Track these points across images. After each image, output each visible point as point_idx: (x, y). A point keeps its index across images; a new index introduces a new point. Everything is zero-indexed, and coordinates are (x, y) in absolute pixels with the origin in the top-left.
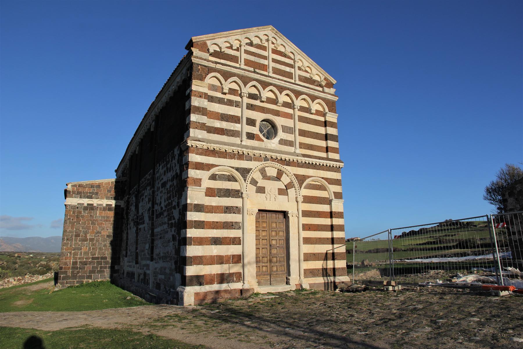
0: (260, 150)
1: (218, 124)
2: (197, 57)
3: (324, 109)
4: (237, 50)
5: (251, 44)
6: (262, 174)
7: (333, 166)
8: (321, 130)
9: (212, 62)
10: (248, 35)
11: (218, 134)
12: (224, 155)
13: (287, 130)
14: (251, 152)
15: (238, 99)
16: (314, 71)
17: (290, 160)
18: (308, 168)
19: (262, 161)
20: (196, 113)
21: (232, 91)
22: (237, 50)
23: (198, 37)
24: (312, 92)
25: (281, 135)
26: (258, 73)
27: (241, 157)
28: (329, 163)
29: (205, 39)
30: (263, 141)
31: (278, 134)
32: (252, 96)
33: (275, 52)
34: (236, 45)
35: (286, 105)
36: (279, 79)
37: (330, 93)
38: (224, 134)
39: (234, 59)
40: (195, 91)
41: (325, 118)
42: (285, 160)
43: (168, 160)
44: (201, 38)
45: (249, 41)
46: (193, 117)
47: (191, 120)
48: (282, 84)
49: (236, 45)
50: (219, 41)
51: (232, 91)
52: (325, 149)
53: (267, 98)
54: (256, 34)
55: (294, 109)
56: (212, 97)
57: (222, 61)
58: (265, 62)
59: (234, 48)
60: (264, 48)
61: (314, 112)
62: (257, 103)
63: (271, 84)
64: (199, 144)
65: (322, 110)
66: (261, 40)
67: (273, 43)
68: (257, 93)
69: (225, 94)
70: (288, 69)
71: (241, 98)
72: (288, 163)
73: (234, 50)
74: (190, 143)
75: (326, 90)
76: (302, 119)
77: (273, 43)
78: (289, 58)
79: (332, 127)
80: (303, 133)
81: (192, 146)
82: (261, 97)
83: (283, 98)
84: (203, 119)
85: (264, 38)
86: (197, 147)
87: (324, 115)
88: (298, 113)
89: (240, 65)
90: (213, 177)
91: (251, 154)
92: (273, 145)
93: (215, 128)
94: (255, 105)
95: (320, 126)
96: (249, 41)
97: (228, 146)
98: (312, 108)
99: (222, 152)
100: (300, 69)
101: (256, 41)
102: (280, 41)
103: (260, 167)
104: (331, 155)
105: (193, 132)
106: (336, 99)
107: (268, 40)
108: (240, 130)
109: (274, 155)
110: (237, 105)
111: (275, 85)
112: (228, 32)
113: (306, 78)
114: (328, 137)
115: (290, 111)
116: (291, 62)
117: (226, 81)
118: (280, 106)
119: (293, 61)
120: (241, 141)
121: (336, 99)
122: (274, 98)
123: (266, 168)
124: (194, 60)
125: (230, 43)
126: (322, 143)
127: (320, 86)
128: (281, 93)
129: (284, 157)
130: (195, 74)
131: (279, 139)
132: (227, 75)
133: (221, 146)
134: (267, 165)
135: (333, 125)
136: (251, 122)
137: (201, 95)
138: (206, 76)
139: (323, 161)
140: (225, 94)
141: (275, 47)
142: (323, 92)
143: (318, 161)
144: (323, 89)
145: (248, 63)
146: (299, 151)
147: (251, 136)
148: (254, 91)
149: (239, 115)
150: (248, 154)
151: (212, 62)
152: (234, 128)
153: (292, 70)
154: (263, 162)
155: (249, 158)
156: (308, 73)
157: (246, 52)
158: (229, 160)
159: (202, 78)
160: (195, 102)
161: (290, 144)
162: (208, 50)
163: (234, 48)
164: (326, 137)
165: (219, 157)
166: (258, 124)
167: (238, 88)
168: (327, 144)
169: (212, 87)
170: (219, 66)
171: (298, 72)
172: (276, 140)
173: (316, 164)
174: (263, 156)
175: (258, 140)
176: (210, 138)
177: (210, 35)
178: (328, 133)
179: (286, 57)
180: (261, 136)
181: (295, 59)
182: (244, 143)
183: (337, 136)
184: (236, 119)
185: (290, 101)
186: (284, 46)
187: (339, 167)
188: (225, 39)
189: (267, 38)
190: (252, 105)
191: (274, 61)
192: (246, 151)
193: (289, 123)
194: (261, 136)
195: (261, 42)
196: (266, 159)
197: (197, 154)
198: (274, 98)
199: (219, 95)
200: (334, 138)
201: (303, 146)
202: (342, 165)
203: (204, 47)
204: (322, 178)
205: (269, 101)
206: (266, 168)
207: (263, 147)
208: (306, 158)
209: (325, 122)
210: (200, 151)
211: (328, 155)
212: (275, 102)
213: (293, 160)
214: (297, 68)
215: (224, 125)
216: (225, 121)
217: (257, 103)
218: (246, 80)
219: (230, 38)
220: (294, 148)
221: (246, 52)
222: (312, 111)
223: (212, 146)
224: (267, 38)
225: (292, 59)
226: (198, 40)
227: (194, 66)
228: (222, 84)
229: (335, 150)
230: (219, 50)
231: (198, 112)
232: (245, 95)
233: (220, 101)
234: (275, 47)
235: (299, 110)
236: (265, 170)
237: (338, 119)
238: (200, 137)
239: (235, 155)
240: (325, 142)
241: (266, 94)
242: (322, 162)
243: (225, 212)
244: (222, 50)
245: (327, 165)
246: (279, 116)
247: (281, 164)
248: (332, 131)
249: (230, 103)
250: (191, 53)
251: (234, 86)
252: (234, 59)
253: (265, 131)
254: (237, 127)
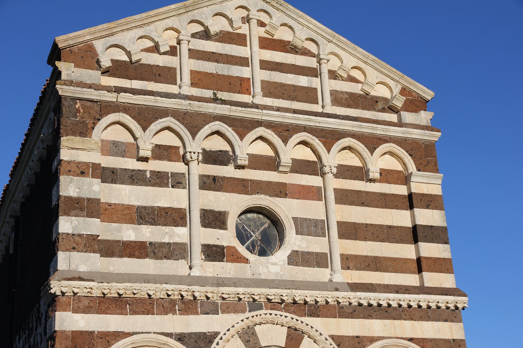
0: (235, 285)
1: (129, 233)
2: (71, 83)
3: (404, 164)
4: (173, 51)
5: (206, 35)
7: (438, 308)
8: (401, 218)
9: (109, 89)
10: (196, 14)
11: (131, 256)
12: (145, 306)
13: (308, 227)
14: (214, 293)
15: (179, 167)
16: (373, 76)
17: (317, 302)
18: (369, 317)
19: (244, 312)
20: (73, 212)
21: (162, 152)
22: (173, 51)
23: (71, 35)
24: (366, 128)
25: (294, 241)
26: (224, 102)
27: (189, 306)
28: (424, 300)
29: (88, 37)
30: (246, 261)
31: (287, 239)
32: (212, 157)
33: (267, 43)
34: (167, 40)
35: (300, 167)
36: (278, 109)
37: (418, 125)
38: (146, 256)
39: (167, 75)
40: (69, 162)
41: (409, 188)
42: (306, 303)
43: (31, 326)
44: (79, 37)
45: (201, 28)
46: (66, 225)
47: (61, 230)
48: (289, 119)
49: (167, 40)
50: (126, 38)
51: (162, 152)
52: (415, 265)
53: (252, 157)
54: (217, 9)
55: (323, 175)
56: (113, 171)
57: (136, 84)
58: (244, 72)
59: (162, 50)
60: (240, 40)
61: (377, 176)
62: (228, 171)
63: (259, 123)
64: (81, 288)
65: (400, 168)
66: (231, 21)
67: (262, 24)
68: (228, 148)
69: (145, 159)
70: (303, 81)
71: (187, 164)
72: (315, 310)
73: (165, 53)
74: (56, 286)
75: (408, 117)
76: (344, 197)
77: (262, 24)
78: (306, 52)
79: (428, 207)
80: (349, 231)
81: (63, 294)
82: (235, 158)
83: (292, 151)
84: (93, 226)
85: (237, 15)
86: (75, 294)
87: (405, 179)
88: (334, 183)
89: (180, 87)
91: (215, 298)
92: (274, 269)
93: (124, 243)
94: (224, 178)
95: (396, 207)
96: (201, 28)
97: (155, 283)
98: (370, 166)
99: (141, 301)
100: (333, 75)
101: (217, 25)
102: (278, 17)
103: (238, 327)
104: (431, 279)
105: (64, 260)
106: (434, 136)
107: (247, 20)
108: (186, 240)
109: (274, 293)
110: (178, 181)
111: (269, 125)
112: (144, 15)
113: (352, 96)
114: (420, 234)
115: (314, 181)
116: (312, 62)
117: (144, 129)
118: (286, 173)
119: (315, 59)
120: (190, 268)
121: (434, 136)
122: (271, 153)
123: (257, 328)
124: (62, 90)
125: (152, 40)
126: (407, 251)
127: (392, 109)
128: (285, 141)
129: (300, 295)
130: (66, 121)
131: (288, 252)
132: (145, 116)
133: (137, 286)
134: (257, 320)
135: (430, 202)
136: (214, 219)
137: (82, 170)
138: (95, 124)
139: (407, 296)
140: (145, 159)
141: (267, 32)
142: (400, 124)
143: (394, 299)
144: (400, 118)
145: (199, 79)
146: (342, 276)
147: (214, 253)
148: (217, 144)
149: (184, 205)
150: (208, 298)
151: (109, 89)
152: (171, 237)
153: (315, 82)
154: (248, 314)
155: (211, 308)
156: (357, 81)
157: (194, 54)
158: (157, 318)
159: (84, 131)
160: (69, 187)
161: (320, 260)
162: (98, 62)
163: (162, 50)
164: (416, 234)
165: (134, 312)
166: (232, 222)
167: (177, 143)
168: (417, 251)
169: (114, 148)
170: (125, 98)
171: (331, 85)
172: (281, 256)
173: (389, 305)
174: (246, 299)
175: (233, 261)
176: (111, 269)
177: (100, 27)
178: (417, 223)
179: (296, 53)
180: (242, 250)
181: (319, 54)
182: (195, 272)
183: (444, 230)
184: (176, 217)
185: (312, 158)
186: (291, 28)
187: (457, 308)
188: (140, 32)
189: (244, 13)
190: (215, 179)
191: (266, 65)
192: (199, 291)
193: (313, 210)
194: (242, 250)
195: (232, 27)
196: (255, 305)
197: (76, 311)
198: (271, 153)
199: (132, 164)
200: (436, 235)
201: (349, 262)
202: (461, 301)
203: (87, 57)
204: (411, 340)
205: (257, 162)
206: (257, 328)
207: (248, 275)
208: (359, 294)
209: (410, 196)
210: (86, 302)
211: (422, 280)
212: (272, 163)
213: (327, 302)
214: (325, 75)
215: (147, 233)
216: (147, 223)
217: (228, 171)
218: (194, 123)
219: (152, 27)
220: (328, 271)
221: (194, 54)
222: (372, 175)
223: (113, 289)
224: (244, 13)
225: (314, 56)
226: (71, 42)
227: (65, 103)
228: (135, 139)
229: (441, 265)
230: (125, 58)
231: (76, 211)
232: (195, 156)
233: (135, 178)
234: (267, 32)
235: (336, 176)
236: (254, 334)
237: (443, 185)
238: (83, 268)
239: (173, 303)
240: (412, 247)
241: (248, 147)
242: (405, 299)
244: (134, 58)
245: (420, 307)
246: (285, 196)
247: (294, 313)
248: (427, 217)
249: (159, 179)
250: (56, 75)
251: (168, 139)
252: (167, 75)
253: (256, 236)
254: (178, 234)
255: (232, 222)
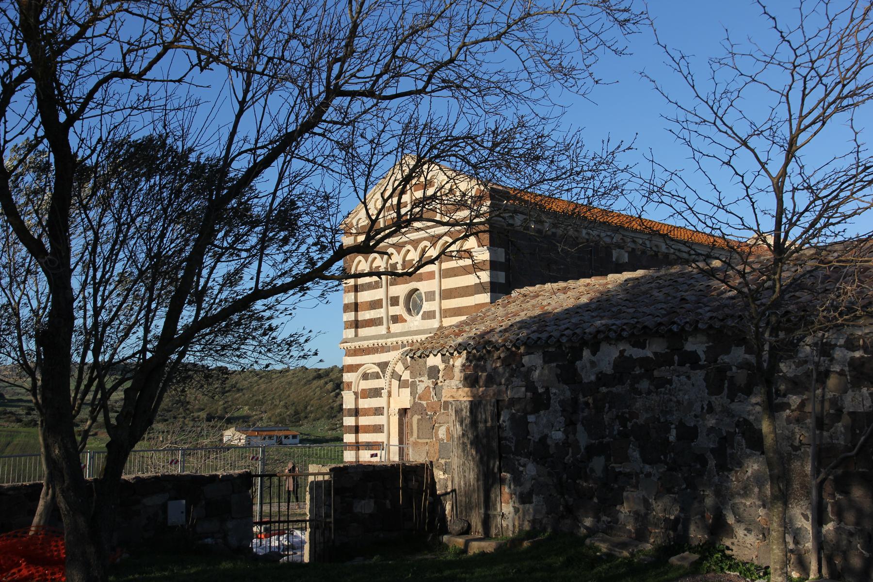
6: (403, 364)
13: (430, 296)
25: (427, 306)
90: (365, 377)
92: (416, 323)
136: (394, 301)
147: (396, 319)
166: (401, 301)
180: (406, 315)
194: (406, 315)
243: (375, 414)
255: (401, 301)
